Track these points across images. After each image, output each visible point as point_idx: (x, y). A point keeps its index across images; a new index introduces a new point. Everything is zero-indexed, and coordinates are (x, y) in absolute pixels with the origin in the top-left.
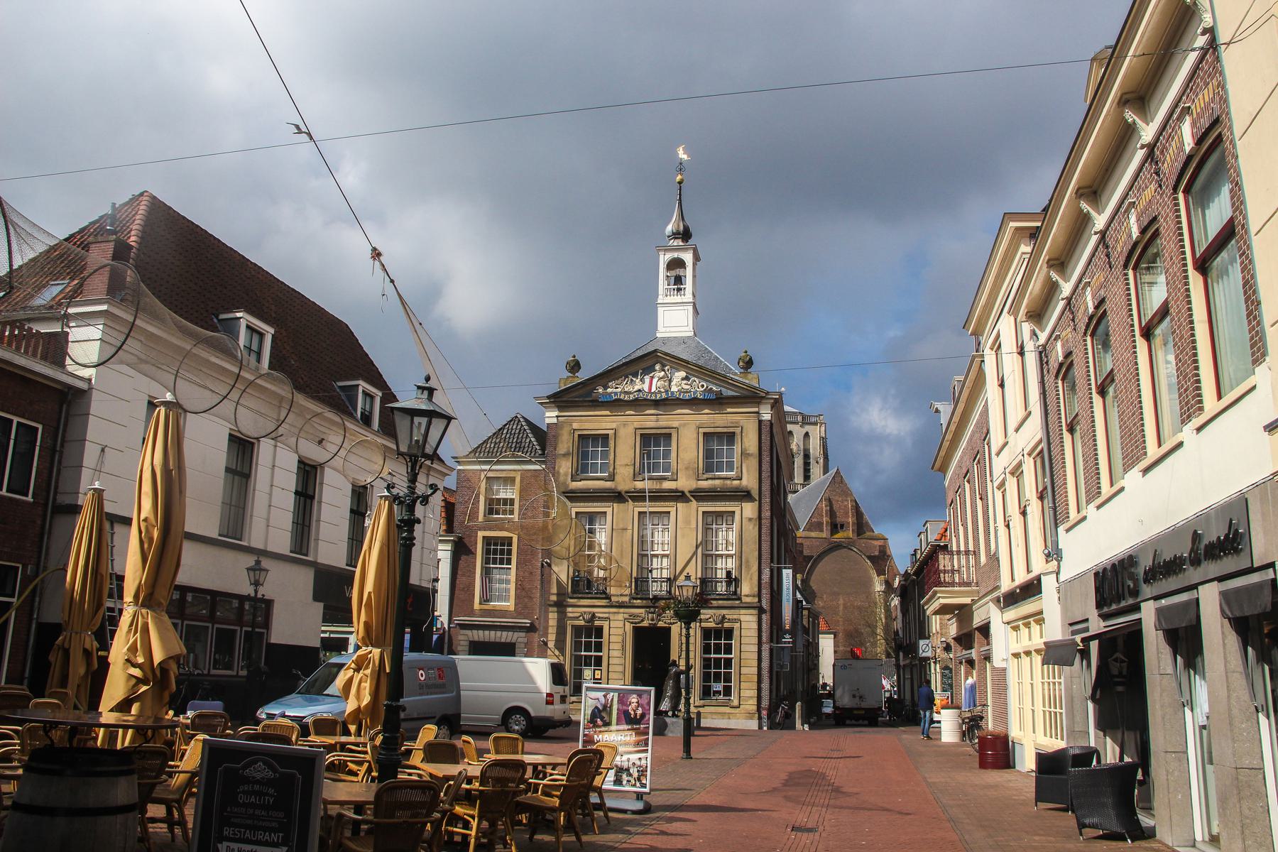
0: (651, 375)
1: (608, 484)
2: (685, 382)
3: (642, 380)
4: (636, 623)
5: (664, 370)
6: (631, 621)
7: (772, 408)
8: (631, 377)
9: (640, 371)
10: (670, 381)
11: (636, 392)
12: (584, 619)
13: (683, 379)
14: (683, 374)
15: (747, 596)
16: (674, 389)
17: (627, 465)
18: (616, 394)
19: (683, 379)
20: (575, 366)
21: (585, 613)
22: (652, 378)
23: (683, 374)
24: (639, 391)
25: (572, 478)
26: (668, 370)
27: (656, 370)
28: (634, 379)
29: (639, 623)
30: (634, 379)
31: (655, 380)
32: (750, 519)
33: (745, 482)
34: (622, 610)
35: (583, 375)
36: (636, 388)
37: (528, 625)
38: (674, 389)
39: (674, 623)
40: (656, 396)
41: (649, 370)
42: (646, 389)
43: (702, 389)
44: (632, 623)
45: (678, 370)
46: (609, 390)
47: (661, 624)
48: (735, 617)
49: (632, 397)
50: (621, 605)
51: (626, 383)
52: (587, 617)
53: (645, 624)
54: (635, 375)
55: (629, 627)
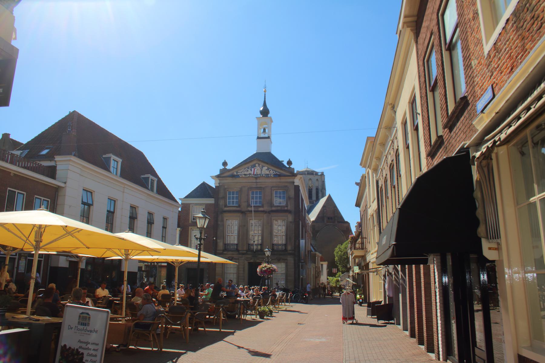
0: (255, 168)
1: (238, 209)
2: (266, 171)
3: (251, 170)
7: (299, 180)
8: (246, 169)
10: (261, 170)
11: (248, 174)
13: (266, 170)
14: (266, 168)
15: (290, 250)
17: (245, 202)
18: (241, 175)
19: (266, 170)
20: (225, 164)
21: (230, 257)
22: (254, 169)
24: (250, 174)
27: (256, 166)
28: (248, 170)
30: (248, 170)
31: (256, 170)
32: (291, 222)
33: (289, 208)
34: (243, 256)
35: (229, 167)
36: (248, 173)
38: (263, 173)
40: (256, 176)
42: (252, 173)
44: (247, 260)
46: (239, 174)
50: (243, 254)
53: (252, 261)
54: (248, 168)
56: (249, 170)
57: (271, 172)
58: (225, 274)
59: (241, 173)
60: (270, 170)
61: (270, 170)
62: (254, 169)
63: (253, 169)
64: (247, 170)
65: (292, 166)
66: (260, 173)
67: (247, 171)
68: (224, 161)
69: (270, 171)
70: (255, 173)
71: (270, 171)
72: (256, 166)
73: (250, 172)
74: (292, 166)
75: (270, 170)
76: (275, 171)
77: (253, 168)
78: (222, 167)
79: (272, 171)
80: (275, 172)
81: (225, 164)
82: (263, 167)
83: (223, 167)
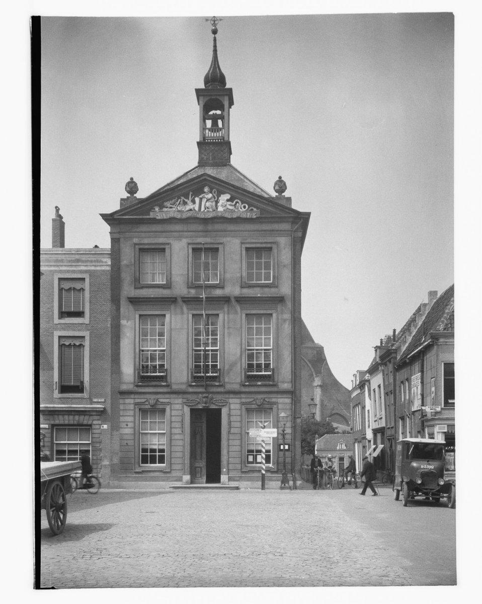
0: (201, 196)
2: (229, 203)
3: (194, 202)
4: (192, 406)
5: (211, 192)
6: (188, 404)
8: (183, 198)
9: (191, 193)
10: (217, 202)
12: (149, 403)
13: (228, 200)
14: (228, 196)
16: (220, 209)
20: (132, 187)
22: (201, 199)
23: (228, 196)
25: (135, 286)
26: (215, 192)
27: (205, 193)
28: (186, 200)
29: (195, 405)
30: (186, 200)
31: (204, 201)
35: (142, 194)
36: (188, 208)
37: (102, 409)
39: (223, 406)
41: (198, 191)
42: (197, 209)
43: (244, 210)
45: (224, 193)
47: (214, 407)
48: (274, 400)
49: (184, 216)
51: (179, 204)
52: (152, 402)
55: (187, 410)
56: (189, 202)
57: (239, 205)
58: (141, 435)
59: (171, 208)
60: (237, 202)
61: (236, 200)
62: (201, 199)
63: (197, 200)
64: (184, 200)
65: (286, 194)
66: (214, 207)
67: (185, 203)
68: (129, 180)
69: (236, 204)
70: (203, 209)
71: (236, 204)
72: (205, 193)
73: (190, 206)
74: (286, 194)
75: (237, 202)
76: (247, 203)
77: (198, 197)
78: (126, 195)
79: (242, 204)
80: (247, 207)
81: (132, 187)
82: (220, 193)
83: (129, 195)
